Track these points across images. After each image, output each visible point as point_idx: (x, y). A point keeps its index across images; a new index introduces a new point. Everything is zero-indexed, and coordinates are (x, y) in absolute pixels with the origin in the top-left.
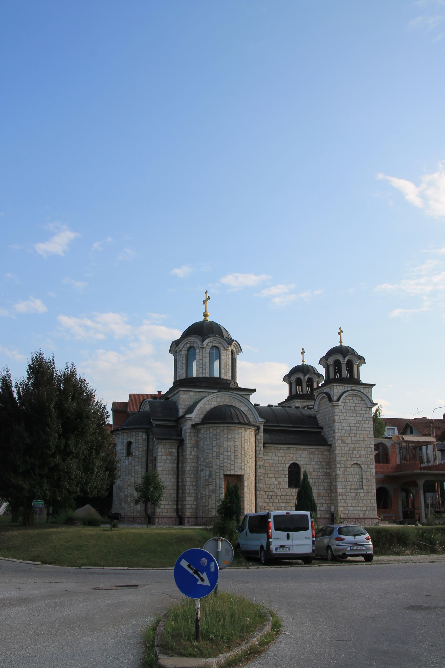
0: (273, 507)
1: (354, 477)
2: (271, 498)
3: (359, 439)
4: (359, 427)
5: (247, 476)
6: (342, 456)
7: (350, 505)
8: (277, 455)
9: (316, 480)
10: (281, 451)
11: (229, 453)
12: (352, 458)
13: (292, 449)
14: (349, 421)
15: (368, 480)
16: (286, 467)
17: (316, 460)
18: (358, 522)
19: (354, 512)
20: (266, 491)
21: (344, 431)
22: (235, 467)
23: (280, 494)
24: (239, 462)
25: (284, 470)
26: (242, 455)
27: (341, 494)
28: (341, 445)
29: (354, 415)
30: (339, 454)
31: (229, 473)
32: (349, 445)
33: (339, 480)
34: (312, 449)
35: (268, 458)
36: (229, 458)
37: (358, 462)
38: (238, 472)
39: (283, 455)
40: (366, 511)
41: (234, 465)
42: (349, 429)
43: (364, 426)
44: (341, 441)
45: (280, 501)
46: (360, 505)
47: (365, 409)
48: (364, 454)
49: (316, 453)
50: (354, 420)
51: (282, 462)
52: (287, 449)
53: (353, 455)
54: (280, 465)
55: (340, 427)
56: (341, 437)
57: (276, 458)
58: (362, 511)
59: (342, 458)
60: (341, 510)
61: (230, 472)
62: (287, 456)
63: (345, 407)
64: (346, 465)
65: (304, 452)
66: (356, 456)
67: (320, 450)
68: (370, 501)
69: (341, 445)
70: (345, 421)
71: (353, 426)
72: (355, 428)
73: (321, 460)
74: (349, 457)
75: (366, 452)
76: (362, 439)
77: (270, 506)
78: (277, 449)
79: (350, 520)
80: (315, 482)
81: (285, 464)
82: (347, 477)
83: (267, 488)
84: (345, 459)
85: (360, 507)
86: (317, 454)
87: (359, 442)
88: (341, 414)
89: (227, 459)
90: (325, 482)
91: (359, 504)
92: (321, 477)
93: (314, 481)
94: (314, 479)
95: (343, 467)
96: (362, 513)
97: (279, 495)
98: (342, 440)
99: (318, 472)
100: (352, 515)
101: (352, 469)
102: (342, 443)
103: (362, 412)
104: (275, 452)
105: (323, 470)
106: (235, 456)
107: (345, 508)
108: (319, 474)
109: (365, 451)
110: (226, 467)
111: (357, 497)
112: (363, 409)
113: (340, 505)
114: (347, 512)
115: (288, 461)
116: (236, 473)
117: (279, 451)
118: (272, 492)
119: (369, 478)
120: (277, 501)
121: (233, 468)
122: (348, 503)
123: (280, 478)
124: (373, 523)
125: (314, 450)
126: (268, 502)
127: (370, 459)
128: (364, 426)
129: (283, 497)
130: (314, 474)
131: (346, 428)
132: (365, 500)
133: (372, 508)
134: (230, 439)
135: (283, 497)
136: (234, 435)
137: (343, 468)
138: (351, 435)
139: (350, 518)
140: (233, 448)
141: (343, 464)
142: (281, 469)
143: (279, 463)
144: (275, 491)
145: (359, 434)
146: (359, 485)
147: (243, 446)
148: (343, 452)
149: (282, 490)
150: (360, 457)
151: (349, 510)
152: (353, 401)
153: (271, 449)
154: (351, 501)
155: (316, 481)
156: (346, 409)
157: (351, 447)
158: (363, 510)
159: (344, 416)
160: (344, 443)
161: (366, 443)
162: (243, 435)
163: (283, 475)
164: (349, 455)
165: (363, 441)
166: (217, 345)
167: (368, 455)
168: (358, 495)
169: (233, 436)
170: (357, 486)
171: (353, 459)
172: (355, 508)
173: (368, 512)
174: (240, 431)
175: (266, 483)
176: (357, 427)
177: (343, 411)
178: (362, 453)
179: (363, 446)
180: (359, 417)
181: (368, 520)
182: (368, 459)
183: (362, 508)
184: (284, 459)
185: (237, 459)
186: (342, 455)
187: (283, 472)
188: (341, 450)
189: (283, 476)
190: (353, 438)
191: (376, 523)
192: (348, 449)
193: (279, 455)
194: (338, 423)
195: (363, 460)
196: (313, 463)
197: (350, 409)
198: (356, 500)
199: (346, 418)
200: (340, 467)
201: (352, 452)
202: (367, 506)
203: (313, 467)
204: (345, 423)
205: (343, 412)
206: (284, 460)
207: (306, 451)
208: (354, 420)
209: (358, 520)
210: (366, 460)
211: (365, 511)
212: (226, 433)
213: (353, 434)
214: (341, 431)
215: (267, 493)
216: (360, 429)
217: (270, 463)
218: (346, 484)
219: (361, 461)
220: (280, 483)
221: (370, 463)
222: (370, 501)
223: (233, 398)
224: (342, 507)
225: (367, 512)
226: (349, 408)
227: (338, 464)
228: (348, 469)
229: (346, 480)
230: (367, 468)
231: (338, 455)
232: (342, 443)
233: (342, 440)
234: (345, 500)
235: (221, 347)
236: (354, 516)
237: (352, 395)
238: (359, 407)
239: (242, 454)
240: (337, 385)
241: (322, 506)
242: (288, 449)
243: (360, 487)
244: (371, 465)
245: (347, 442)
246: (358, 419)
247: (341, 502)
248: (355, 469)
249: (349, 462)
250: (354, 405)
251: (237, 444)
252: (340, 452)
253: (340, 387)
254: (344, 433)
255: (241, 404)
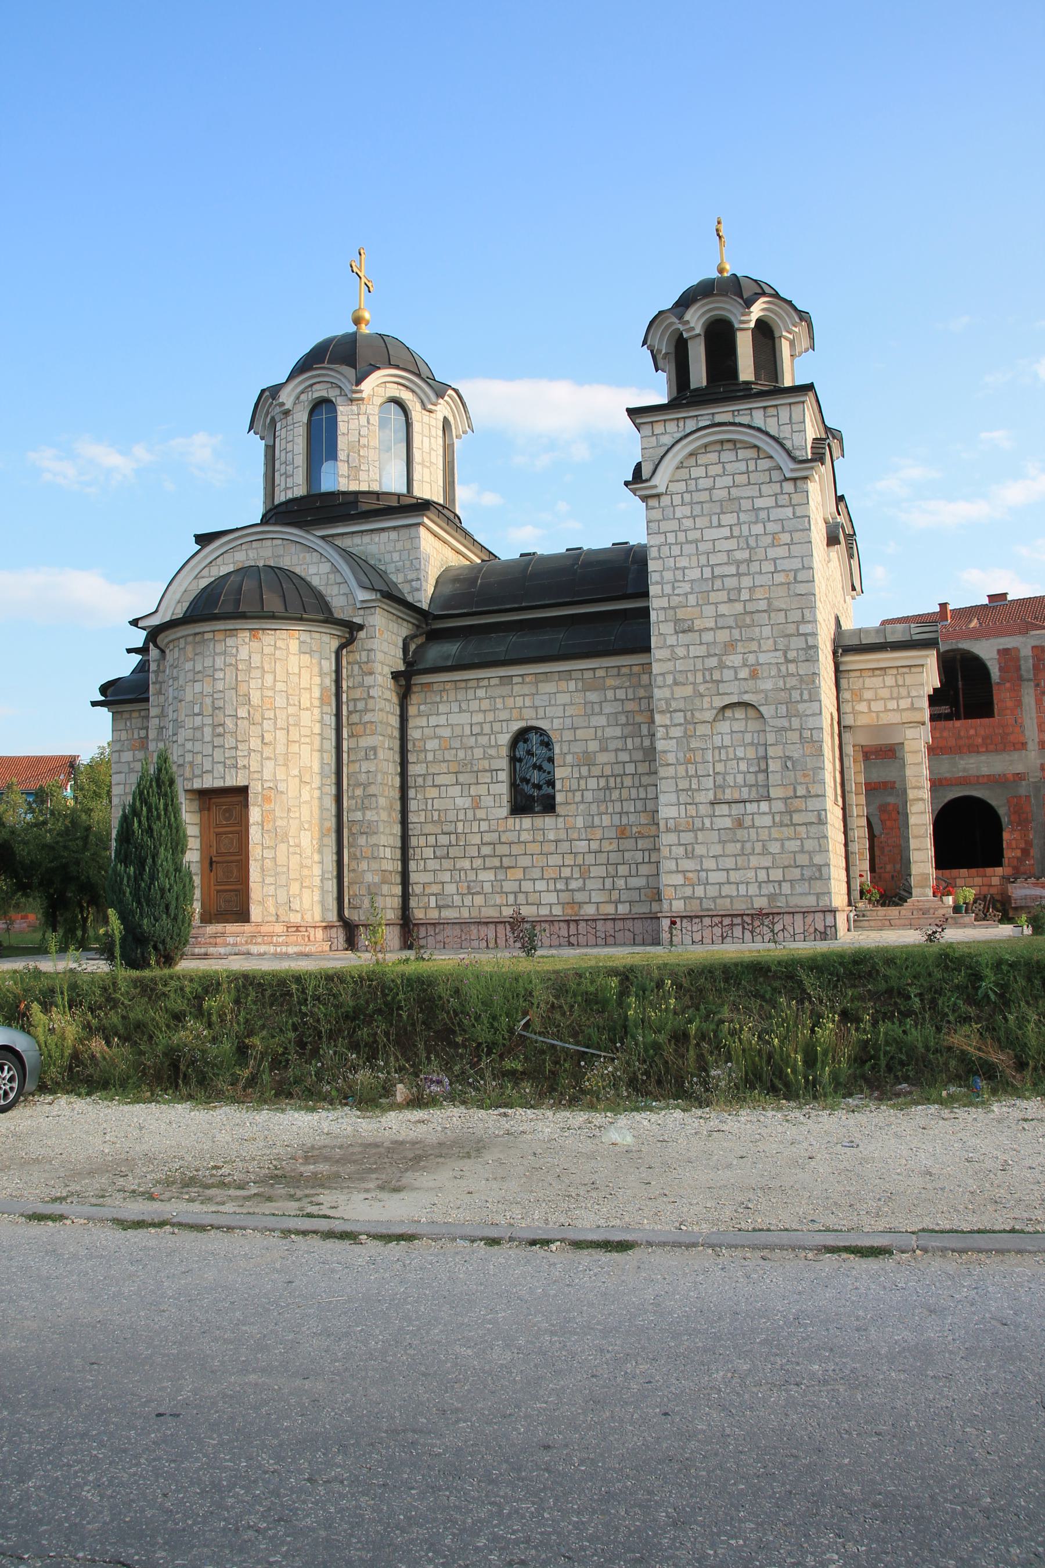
0: (455, 885)
1: (731, 756)
2: (447, 857)
3: (750, 607)
4: (750, 561)
5: (263, 789)
6: (676, 683)
7: (710, 864)
8: (464, 706)
9: (612, 780)
10: (481, 693)
11: (198, 720)
12: (721, 685)
13: (519, 680)
14: (703, 547)
15: (789, 764)
16: (497, 746)
17: (608, 709)
18: (744, 928)
19: (726, 890)
20: (427, 832)
21: (686, 587)
22: (213, 762)
23: (476, 839)
24: (227, 746)
25: (492, 757)
26: (239, 722)
27: (671, 824)
28: (671, 640)
29: (729, 519)
30: (663, 674)
31: (208, 782)
32: (708, 637)
33: (663, 772)
34: (594, 669)
35: (433, 721)
36: (198, 734)
37: (746, 698)
38: (224, 778)
39: (486, 704)
40: (780, 885)
41: (212, 755)
42: (707, 573)
43: (772, 553)
44: (672, 624)
45: (478, 863)
46: (754, 861)
47: (776, 488)
48: (773, 661)
49: (610, 682)
50: (726, 538)
51: (482, 729)
52: (501, 684)
53: (725, 671)
54: (476, 740)
55: (668, 576)
56: (671, 612)
57: (465, 718)
58: (763, 885)
59: (675, 688)
60: (675, 886)
61: (199, 780)
62: (500, 706)
63: (687, 497)
64: (693, 714)
65: (563, 685)
66: (736, 673)
67: (624, 670)
68: (798, 843)
69: (671, 640)
70: (690, 549)
71: (725, 560)
72: (733, 570)
73: (630, 706)
74: (705, 682)
75: (780, 654)
76: (763, 605)
77: (443, 883)
78: (466, 688)
79: (707, 921)
80: (607, 788)
81: (493, 737)
82: (699, 759)
83: (433, 821)
84: (688, 690)
85: (756, 869)
86: (615, 688)
87: (748, 621)
88: (673, 525)
89: (193, 740)
90: (646, 786)
91: (751, 857)
92: (630, 769)
93: (602, 782)
94: (602, 776)
95: (682, 721)
96: (764, 891)
97: (473, 842)
98: (677, 621)
99: (617, 750)
100: (718, 901)
101: (724, 727)
102: (676, 633)
103: (759, 503)
104: (459, 697)
105: (638, 740)
106: (214, 726)
107: (690, 875)
108: (624, 757)
109: (776, 650)
110: (191, 763)
111: (741, 834)
112: (766, 489)
113: (668, 865)
114: (699, 891)
115: (504, 724)
116: (219, 784)
117: (471, 692)
118: (449, 834)
119: (796, 755)
120: (466, 864)
121: (210, 769)
122: (702, 857)
123: (478, 783)
124: (812, 930)
125: (600, 673)
126: (434, 871)
127: (801, 681)
128: (772, 553)
129: (486, 850)
130: (602, 758)
131: (694, 574)
132: (776, 840)
133: (807, 873)
134: (199, 672)
135: (486, 850)
136: (211, 659)
137: (680, 725)
138: (713, 597)
139: (710, 913)
140: (208, 701)
141: (680, 711)
142: (478, 753)
143: (472, 735)
144: (460, 830)
145: (750, 589)
146: (756, 785)
147: (243, 688)
148: (680, 665)
149: (484, 826)
150: (754, 675)
151: (708, 884)
152: (724, 467)
153: (444, 690)
154: (717, 850)
155: (612, 784)
156: (691, 503)
157: (715, 643)
158: (769, 881)
159: (686, 531)
160: (684, 632)
161: (780, 617)
162: (243, 654)
163: (489, 774)
164: (707, 673)
165: (765, 615)
166: (324, 394)
167: (792, 668)
168: (748, 822)
169: (208, 662)
170: (745, 790)
171: (723, 688)
172: (734, 876)
173: (792, 887)
174: (230, 641)
175: (430, 807)
176: (738, 563)
177: (681, 512)
178: (763, 658)
179: (767, 631)
180: (750, 523)
181: (788, 918)
182: (788, 679)
183: (762, 875)
184: (490, 717)
185: (219, 735)
186: (675, 679)
187: (485, 764)
188: (674, 658)
189: (486, 778)
190: (723, 609)
191: (825, 927)
192: (702, 651)
193: (474, 705)
194: (660, 562)
195: (768, 685)
196: (602, 721)
197: (711, 501)
198: (739, 845)
199: (693, 535)
200: (668, 723)
201: (720, 661)
202: (786, 864)
203: (599, 734)
204: (689, 556)
205: (678, 515)
206: (491, 722)
207: (571, 679)
208: (726, 538)
209: (743, 922)
210: (781, 684)
211: (780, 882)
212: (190, 656)
213: (725, 592)
214: (674, 588)
215: (431, 840)
216: (755, 567)
217: (440, 737)
218: (693, 786)
219: (762, 691)
220: (476, 807)
221: (801, 695)
222: (798, 843)
223: (285, 542)
224: (678, 872)
225: (786, 888)
226: (704, 496)
227: (662, 712)
228: (702, 729)
229: (692, 772)
230: (788, 716)
231: (660, 679)
232: (676, 633)
233: (677, 621)
234: (689, 848)
235: (336, 397)
236: (729, 907)
237: (718, 447)
238: (749, 484)
239: (237, 718)
240: (652, 422)
241: (633, 872)
242: (506, 680)
243: (758, 793)
244: (806, 701)
245: (696, 628)
246: (746, 533)
247: (673, 855)
248: (738, 726)
249: (706, 699)
250: (728, 481)
251: (220, 686)
252: (669, 666)
253: (667, 424)
254: (686, 594)
255: (308, 555)
